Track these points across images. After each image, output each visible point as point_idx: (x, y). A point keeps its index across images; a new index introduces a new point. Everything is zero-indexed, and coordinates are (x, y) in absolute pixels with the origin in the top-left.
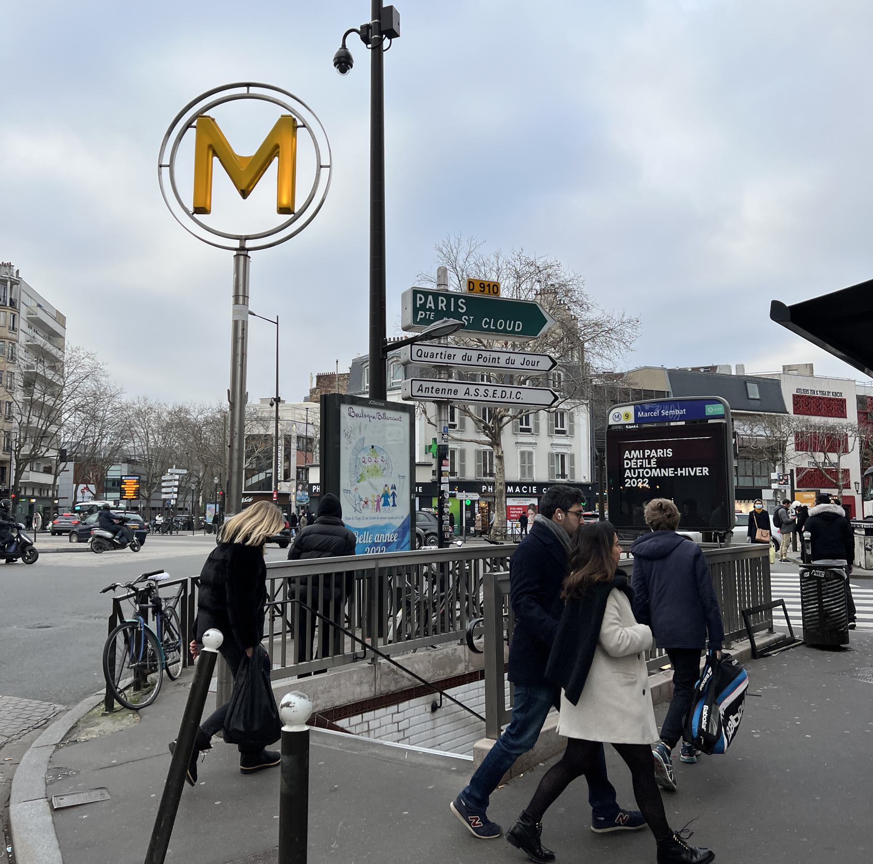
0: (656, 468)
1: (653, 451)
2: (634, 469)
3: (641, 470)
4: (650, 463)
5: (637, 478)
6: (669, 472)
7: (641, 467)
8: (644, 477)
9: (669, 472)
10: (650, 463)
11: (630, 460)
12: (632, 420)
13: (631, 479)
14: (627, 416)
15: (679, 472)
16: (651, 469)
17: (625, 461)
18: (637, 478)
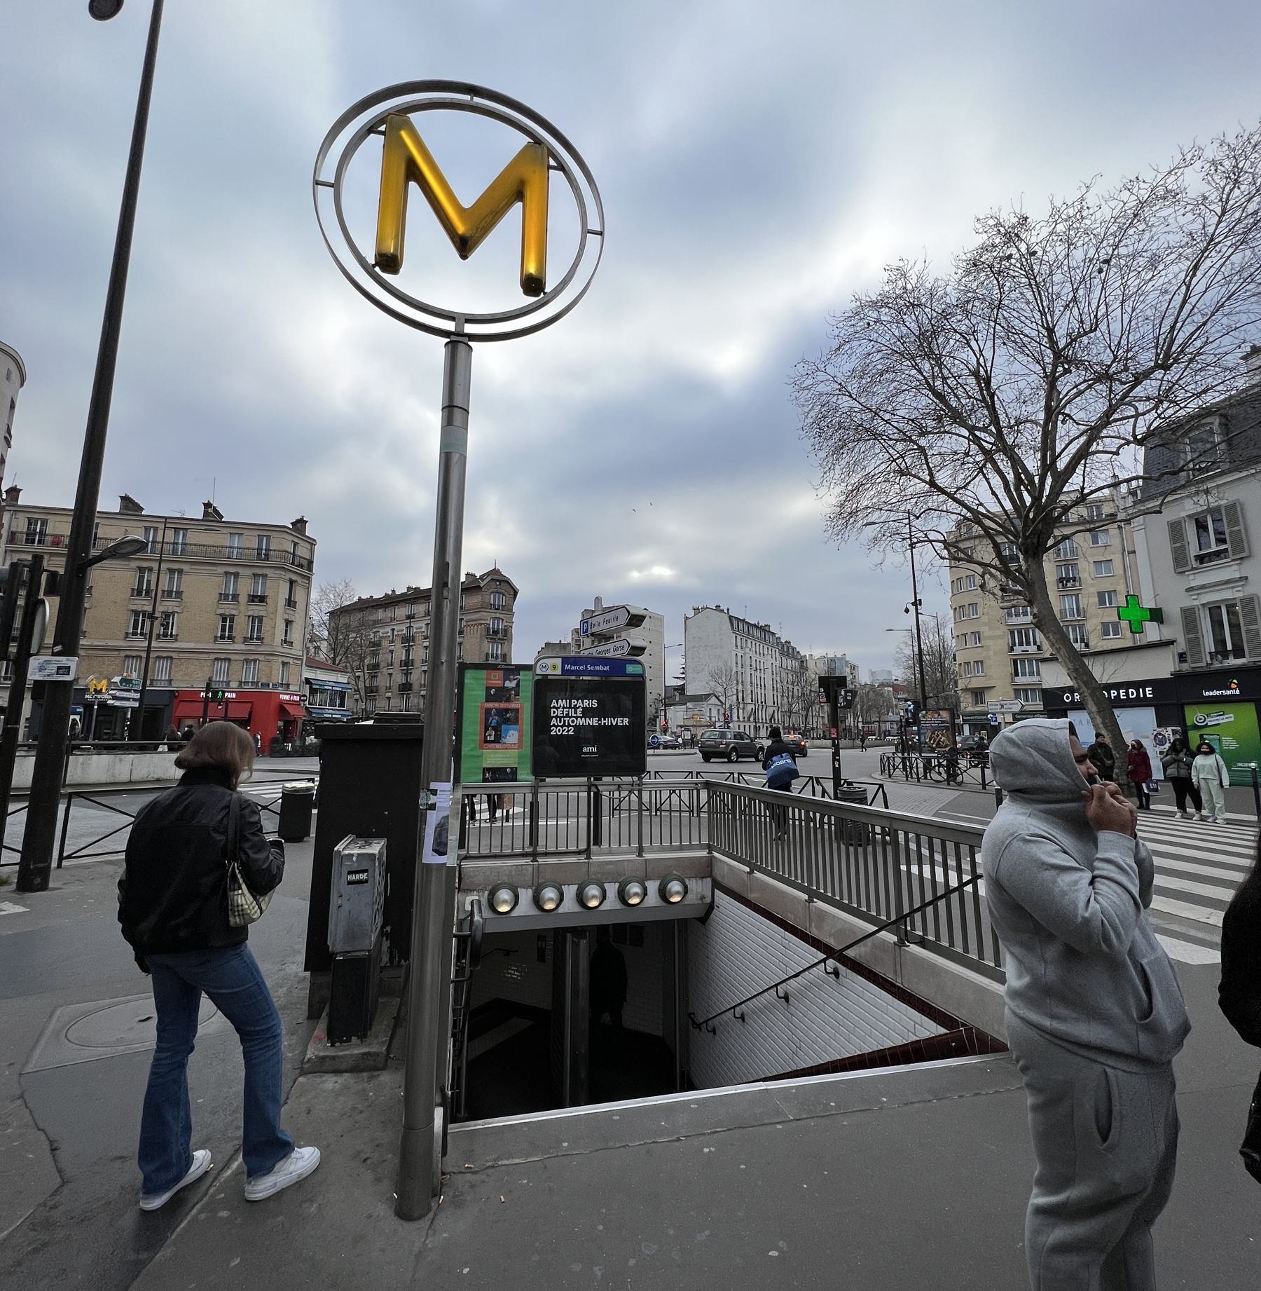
0: (581, 718)
1: (580, 701)
2: (560, 717)
3: (567, 719)
4: (576, 713)
5: (562, 726)
6: (594, 722)
7: (567, 716)
8: (569, 726)
9: (594, 722)
10: (576, 713)
11: (557, 708)
12: (559, 672)
13: (556, 727)
14: (554, 667)
15: (603, 721)
16: (577, 717)
17: (552, 710)
18: (562, 726)
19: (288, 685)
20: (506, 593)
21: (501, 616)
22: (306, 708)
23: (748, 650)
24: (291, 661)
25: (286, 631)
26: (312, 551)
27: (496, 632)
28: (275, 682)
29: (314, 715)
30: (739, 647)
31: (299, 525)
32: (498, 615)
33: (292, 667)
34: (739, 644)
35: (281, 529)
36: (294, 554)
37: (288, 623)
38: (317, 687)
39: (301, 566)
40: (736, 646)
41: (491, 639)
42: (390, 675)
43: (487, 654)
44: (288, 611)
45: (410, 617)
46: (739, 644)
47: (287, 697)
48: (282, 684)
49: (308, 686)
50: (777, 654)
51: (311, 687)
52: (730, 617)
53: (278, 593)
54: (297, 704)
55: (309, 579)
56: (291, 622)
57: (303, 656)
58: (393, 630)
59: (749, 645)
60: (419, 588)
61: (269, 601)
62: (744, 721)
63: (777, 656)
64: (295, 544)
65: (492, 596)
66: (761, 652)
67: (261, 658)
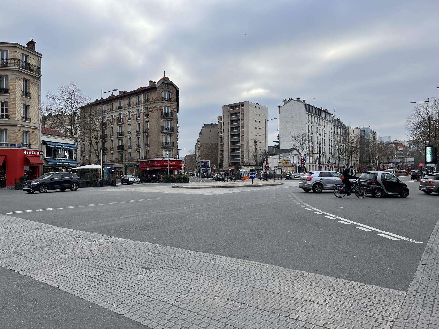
19: (30, 145)
20: (171, 91)
21: (169, 105)
22: (45, 159)
23: (315, 123)
24: (31, 130)
25: (26, 112)
26: (39, 62)
27: (167, 115)
28: (20, 143)
29: (50, 163)
30: (310, 122)
31: (30, 45)
32: (167, 104)
33: (32, 134)
34: (310, 120)
35: (16, 46)
36: (26, 63)
37: (26, 107)
38: (51, 146)
39: (31, 70)
40: (309, 121)
41: (164, 118)
42: (112, 141)
43: (162, 127)
44: (24, 99)
45: (120, 108)
46: (310, 120)
47: (27, 152)
48: (26, 144)
49: (45, 146)
50: (332, 125)
51: (46, 147)
52: (306, 105)
53: (16, 86)
54: (37, 156)
55: (39, 79)
56: (28, 106)
57: (39, 127)
58: (112, 116)
59: (316, 120)
60: (126, 92)
61: (11, 92)
62: (313, 163)
63: (332, 127)
64: (26, 56)
65: (163, 93)
66: (323, 124)
67: (9, 128)
